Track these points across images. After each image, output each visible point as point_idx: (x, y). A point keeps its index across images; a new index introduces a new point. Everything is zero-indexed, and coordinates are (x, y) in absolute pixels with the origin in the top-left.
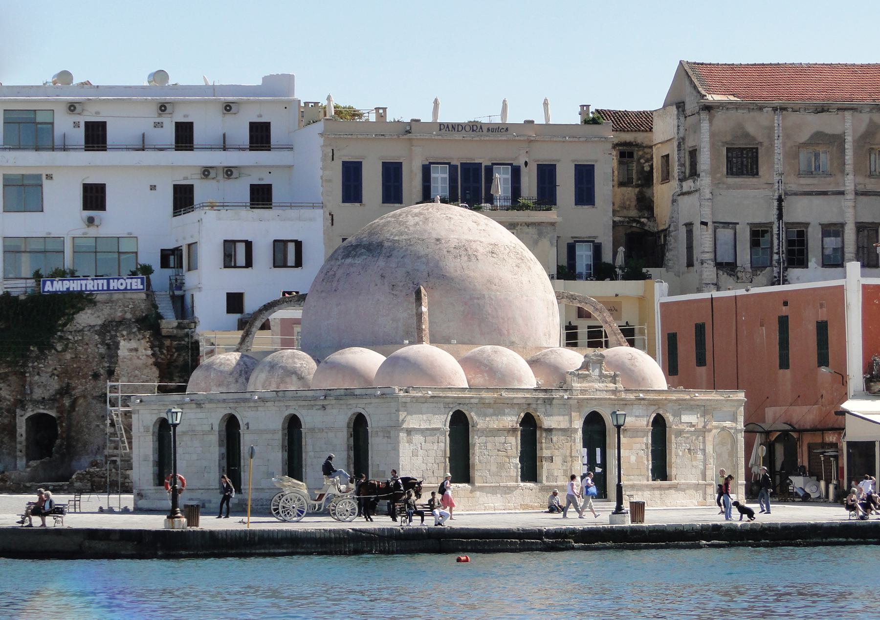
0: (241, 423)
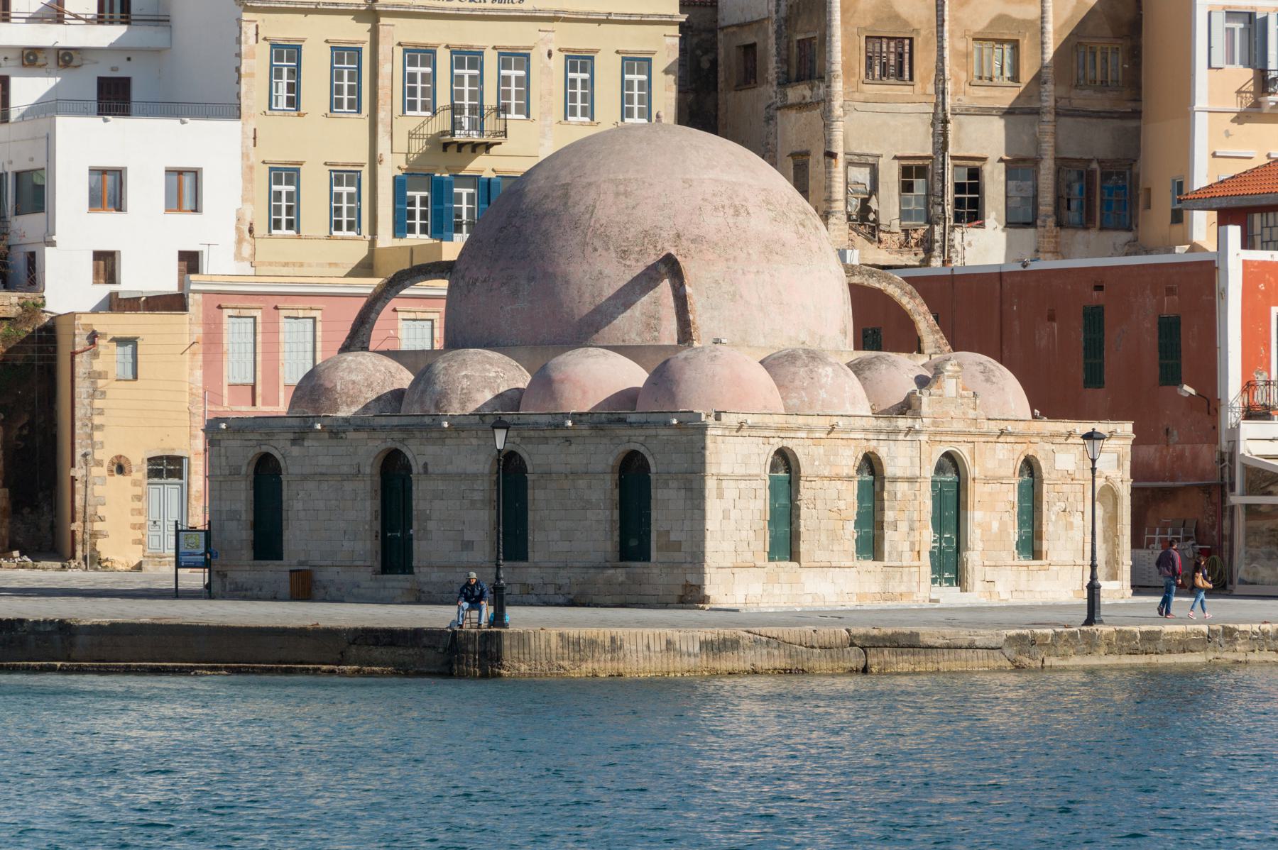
0: (413, 463)
